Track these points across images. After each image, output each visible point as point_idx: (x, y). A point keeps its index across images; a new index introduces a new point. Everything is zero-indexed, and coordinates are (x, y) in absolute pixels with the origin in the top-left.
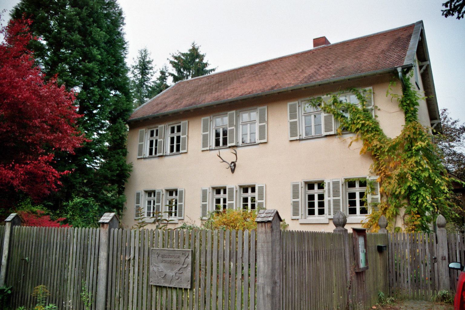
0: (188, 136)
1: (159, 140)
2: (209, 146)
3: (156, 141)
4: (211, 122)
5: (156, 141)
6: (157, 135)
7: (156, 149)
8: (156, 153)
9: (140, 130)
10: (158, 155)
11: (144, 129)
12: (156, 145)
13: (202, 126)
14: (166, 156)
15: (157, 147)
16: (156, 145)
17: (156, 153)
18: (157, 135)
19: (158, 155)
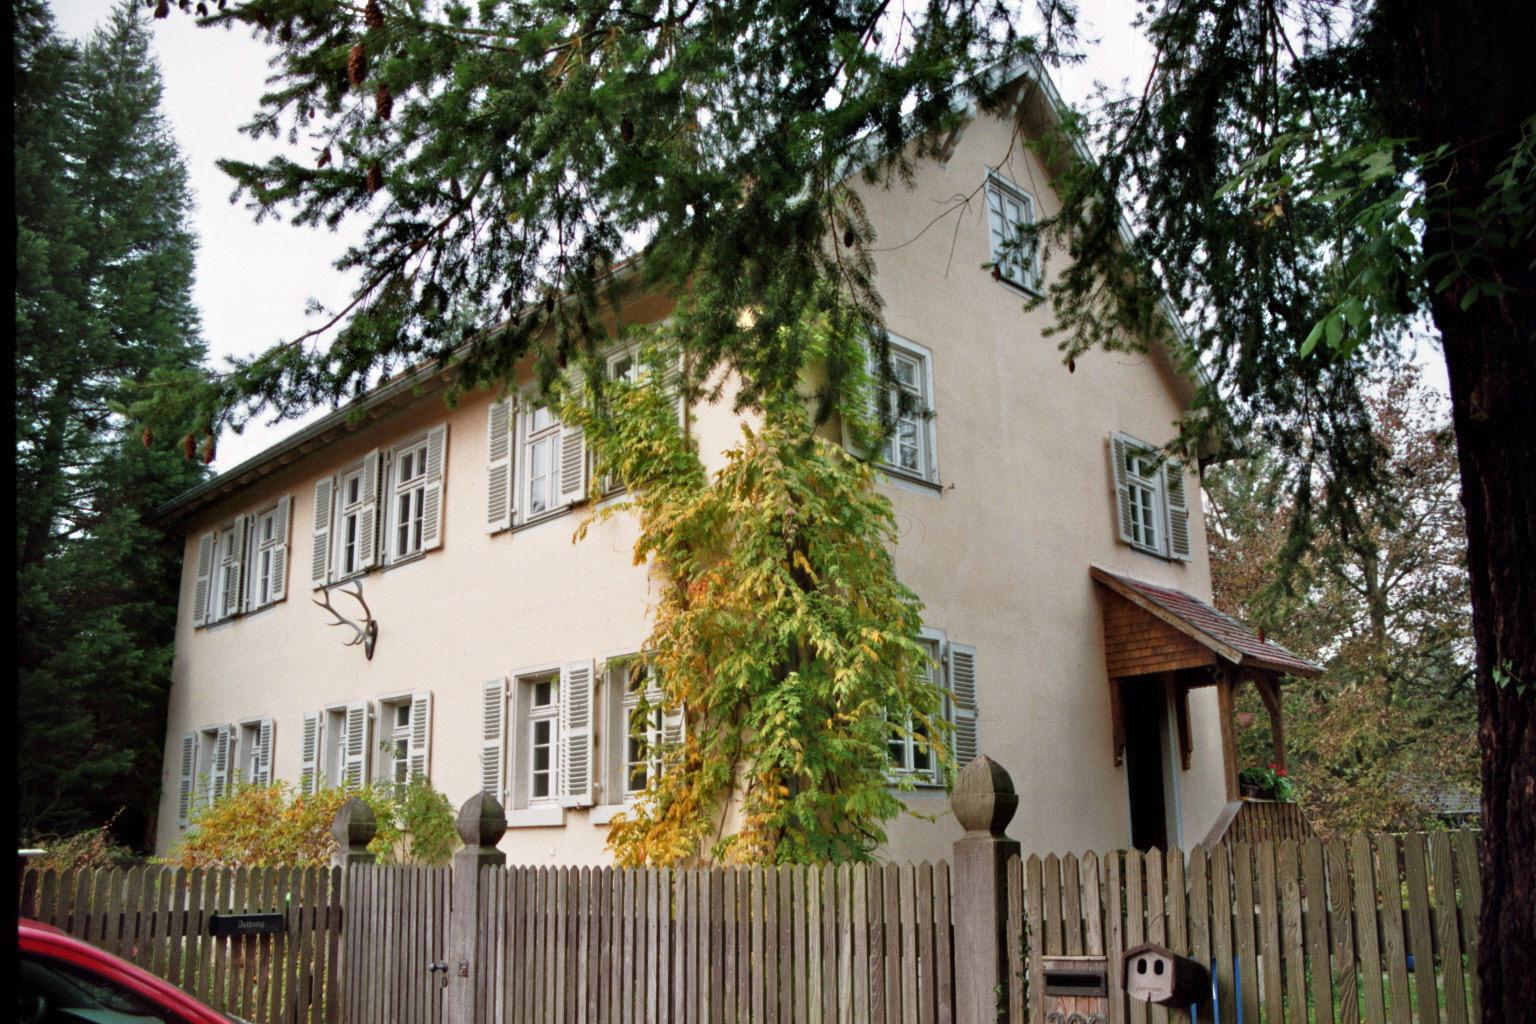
0: (289, 549)
1: (427, 488)
2: (508, 514)
3: (421, 492)
4: (519, 416)
5: (421, 492)
6: (422, 470)
7: (419, 524)
8: (418, 544)
9: (320, 483)
10: (426, 545)
11: (210, 534)
12: (420, 513)
13: (315, 507)
14: (248, 614)
15: (423, 518)
16: (420, 513)
17: (418, 544)
18: (422, 470)
19: (426, 545)
